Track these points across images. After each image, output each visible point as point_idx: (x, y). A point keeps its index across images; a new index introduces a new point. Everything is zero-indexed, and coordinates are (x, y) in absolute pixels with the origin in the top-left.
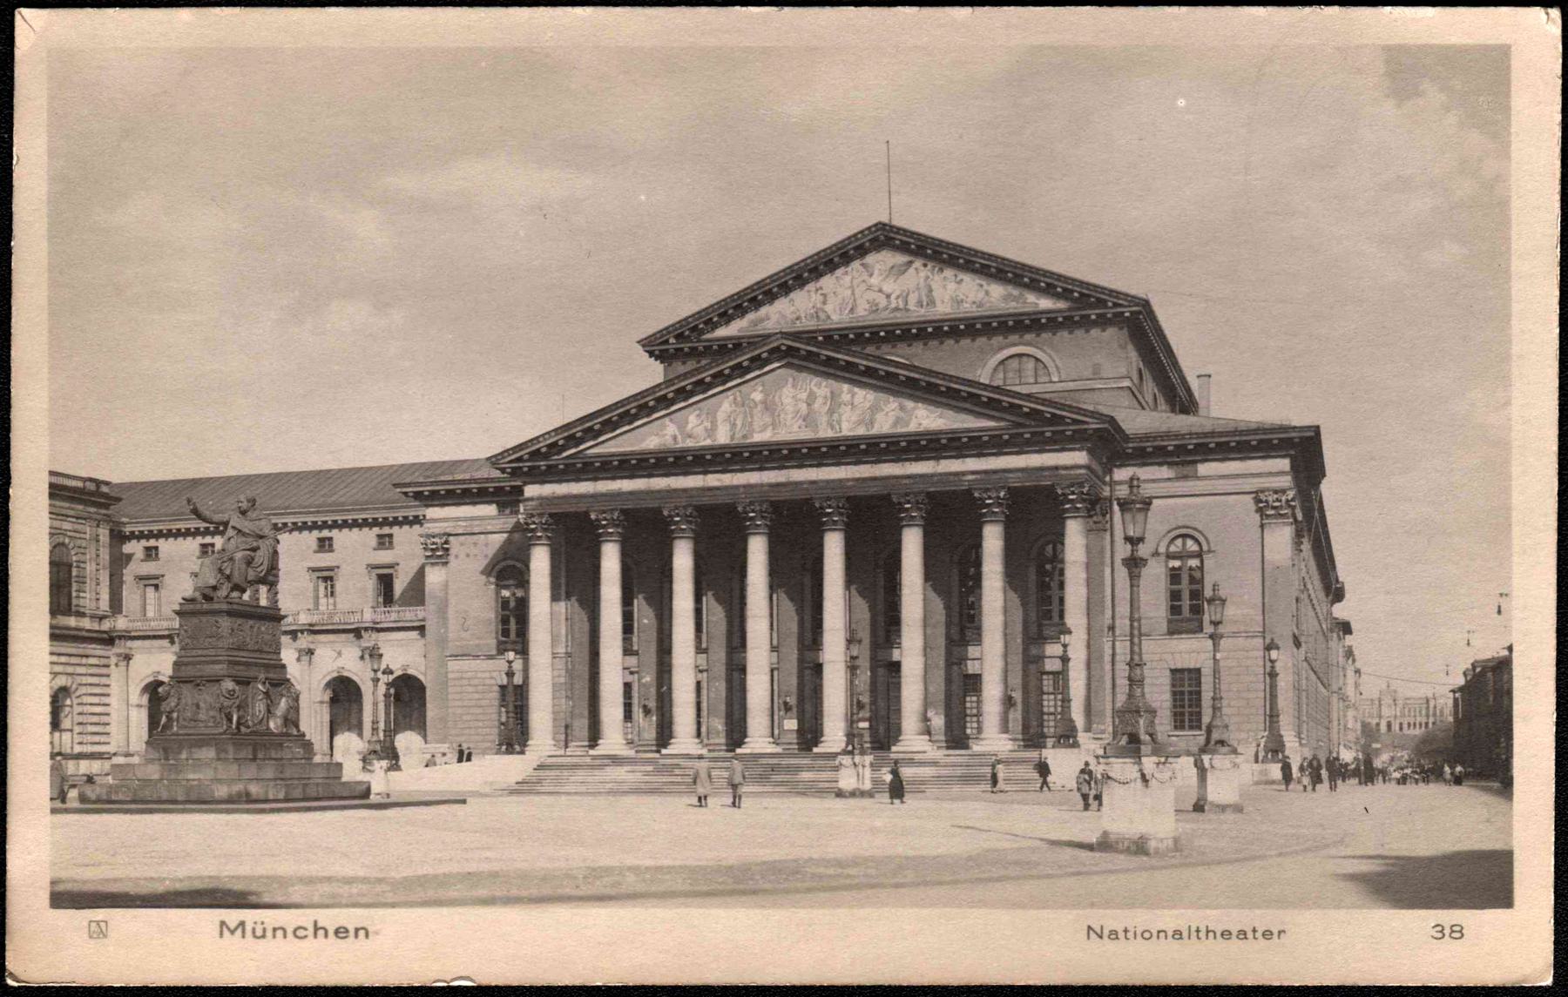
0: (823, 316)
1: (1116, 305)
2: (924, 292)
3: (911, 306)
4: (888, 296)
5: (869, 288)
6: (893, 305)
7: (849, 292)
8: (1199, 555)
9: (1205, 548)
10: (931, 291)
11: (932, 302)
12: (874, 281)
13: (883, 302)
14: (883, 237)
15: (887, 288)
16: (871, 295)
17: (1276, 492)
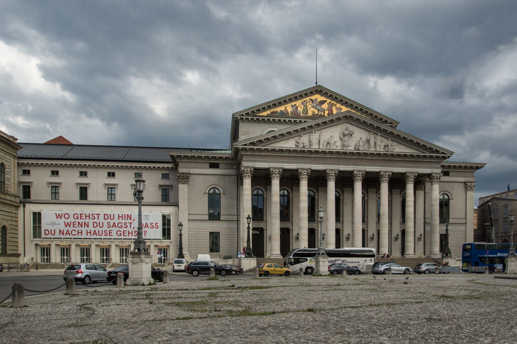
0: (296, 114)
1: (391, 123)
2: (330, 111)
3: (326, 115)
4: (318, 111)
5: (312, 107)
6: (320, 114)
7: (305, 107)
8: (449, 199)
9: (450, 198)
10: (332, 111)
11: (332, 113)
12: (314, 105)
13: (317, 112)
14: (319, 90)
15: (318, 108)
16: (312, 109)
17: (471, 182)
